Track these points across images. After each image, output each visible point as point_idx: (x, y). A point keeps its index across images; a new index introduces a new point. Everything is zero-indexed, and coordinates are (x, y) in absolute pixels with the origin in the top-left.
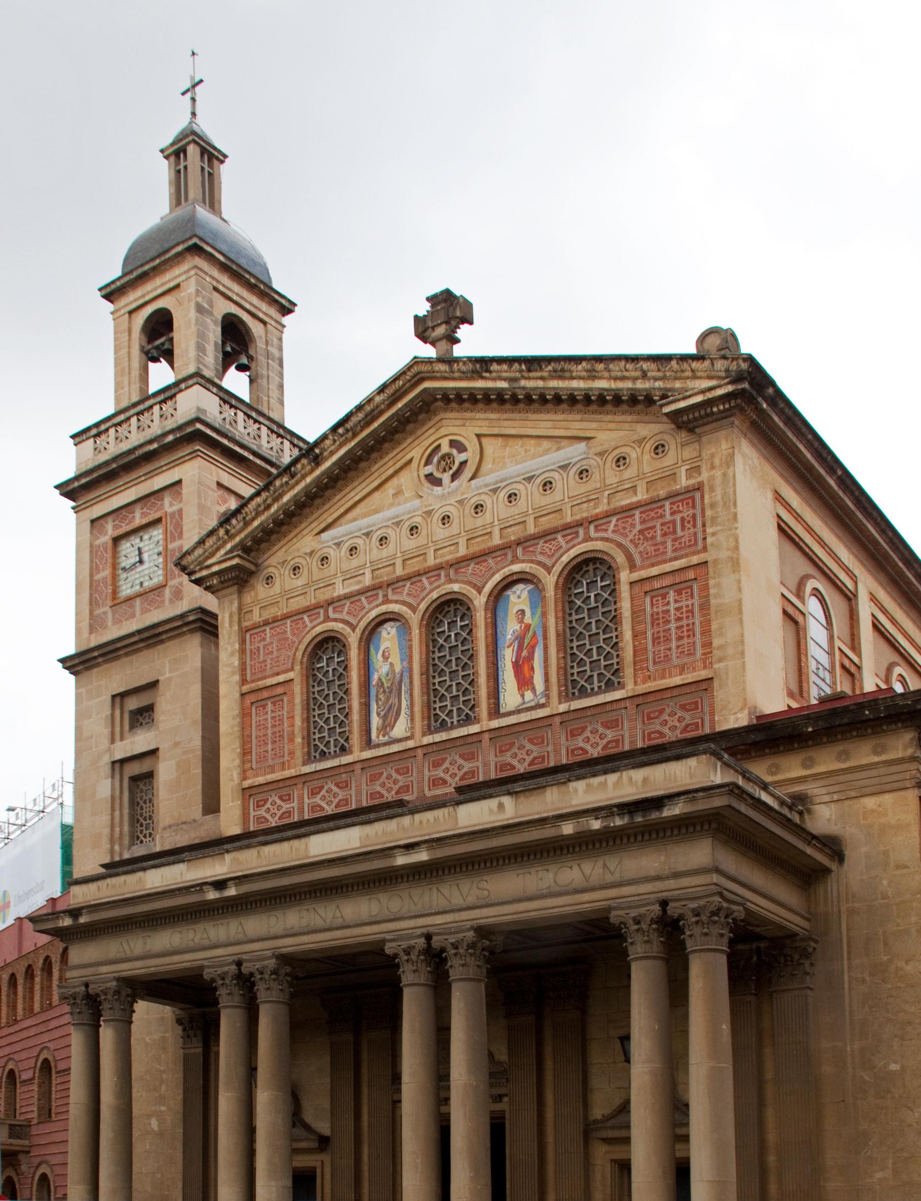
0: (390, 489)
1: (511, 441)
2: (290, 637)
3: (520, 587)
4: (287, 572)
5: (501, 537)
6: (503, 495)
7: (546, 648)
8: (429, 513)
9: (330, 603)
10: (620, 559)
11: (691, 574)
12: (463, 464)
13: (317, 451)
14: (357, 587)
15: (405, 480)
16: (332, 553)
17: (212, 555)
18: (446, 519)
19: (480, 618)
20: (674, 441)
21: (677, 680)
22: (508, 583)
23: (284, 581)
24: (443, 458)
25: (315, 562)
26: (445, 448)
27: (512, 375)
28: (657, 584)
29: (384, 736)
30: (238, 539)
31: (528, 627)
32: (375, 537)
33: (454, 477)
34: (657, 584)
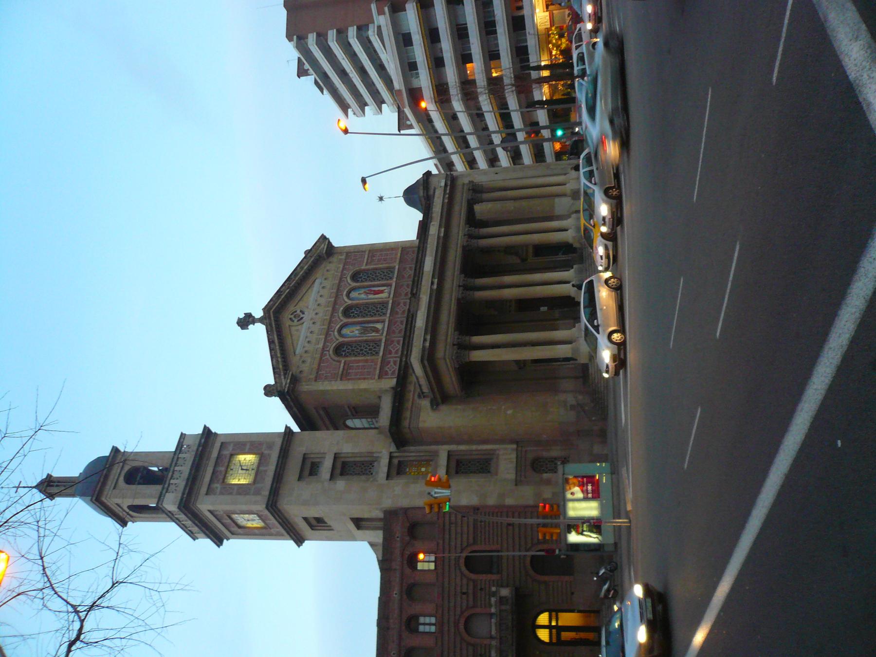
0: (294, 333)
1: (302, 299)
2: (328, 363)
3: (351, 294)
4: (303, 365)
5: (333, 298)
6: (319, 298)
7: (374, 286)
8: (312, 319)
9: (323, 349)
10: (358, 268)
11: (371, 254)
12: (301, 311)
13: (271, 340)
14: (323, 340)
15: (293, 329)
16: (306, 349)
17: (282, 383)
18: (316, 314)
19: (355, 302)
20: (331, 259)
21: (399, 255)
22: (348, 295)
23: (305, 368)
24: (295, 317)
25: (305, 355)
26: (292, 316)
27: (287, 287)
28: (369, 261)
29: (379, 331)
30: (282, 374)
31: (365, 292)
32: (309, 334)
33: (303, 313)
34: (369, 261)
